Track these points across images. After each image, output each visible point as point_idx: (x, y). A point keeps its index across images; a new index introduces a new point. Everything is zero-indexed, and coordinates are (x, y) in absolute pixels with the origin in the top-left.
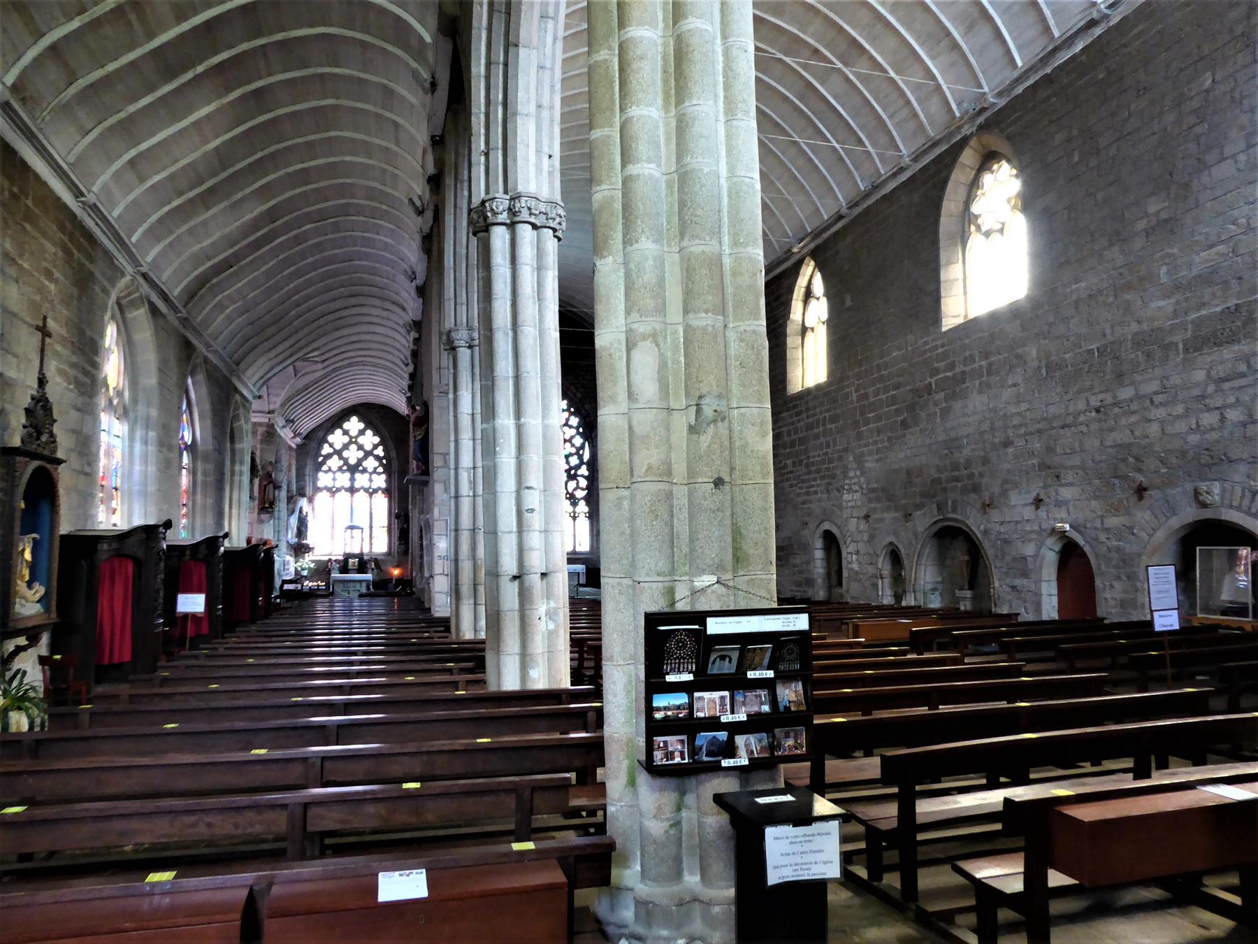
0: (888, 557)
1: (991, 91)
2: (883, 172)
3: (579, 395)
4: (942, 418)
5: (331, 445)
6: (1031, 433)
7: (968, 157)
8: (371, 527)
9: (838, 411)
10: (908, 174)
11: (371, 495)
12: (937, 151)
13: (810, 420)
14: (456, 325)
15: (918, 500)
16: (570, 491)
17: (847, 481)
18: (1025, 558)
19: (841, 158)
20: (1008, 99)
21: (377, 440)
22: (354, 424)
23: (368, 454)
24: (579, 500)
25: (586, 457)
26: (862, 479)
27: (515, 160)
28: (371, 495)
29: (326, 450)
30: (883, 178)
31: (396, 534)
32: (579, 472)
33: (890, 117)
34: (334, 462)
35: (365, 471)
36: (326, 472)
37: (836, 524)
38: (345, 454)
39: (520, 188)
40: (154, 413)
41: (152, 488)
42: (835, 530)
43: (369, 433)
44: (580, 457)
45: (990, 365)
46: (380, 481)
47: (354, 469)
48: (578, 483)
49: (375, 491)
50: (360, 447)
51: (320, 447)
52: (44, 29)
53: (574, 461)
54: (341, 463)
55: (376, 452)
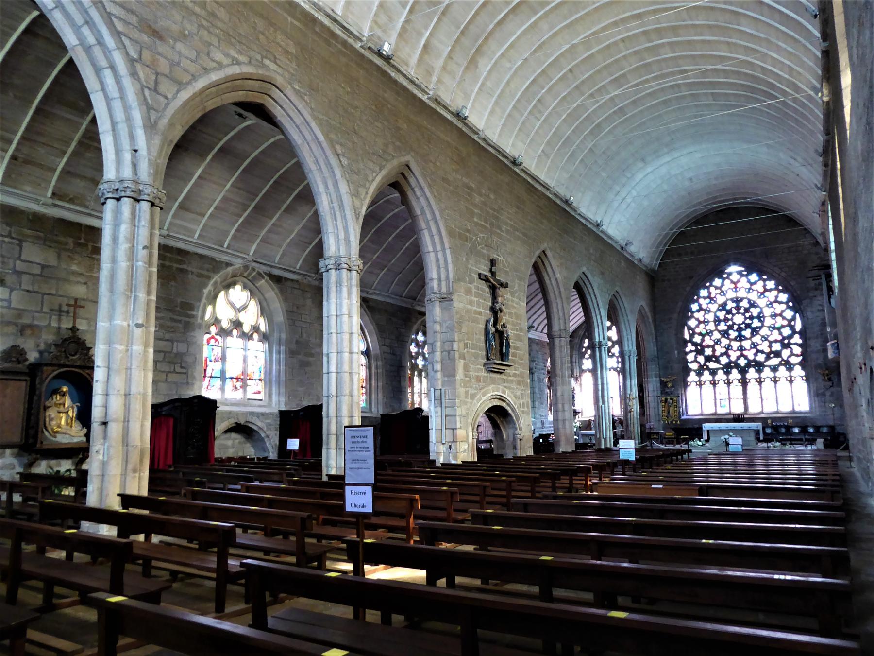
3: (783, 274)
16: (785, 359)
24: (794, 365)
25: (798, 326)
32: (792, 341)
40: (284, 336)
41: (283, 378)
44: (792, 328)
48: (791, 351)
52: (54, 167)
53: (787, 332)
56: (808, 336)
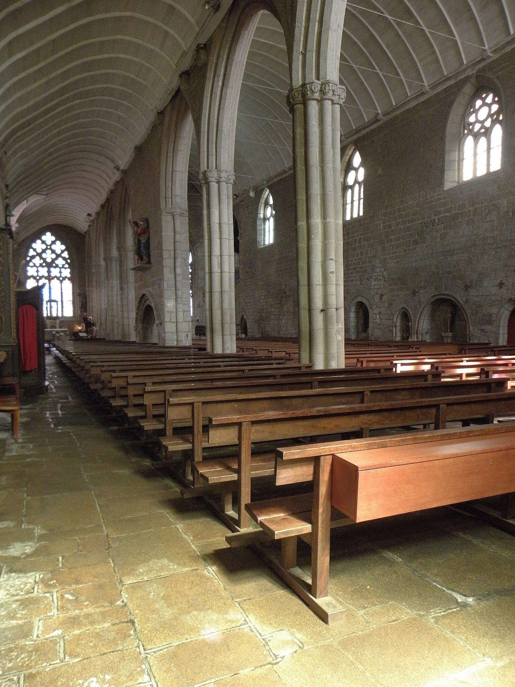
0: (400, 315)
1: (490, 48)
2: (409, 95)
4: (441, 239)
5: (35, 250)
6: (500, 248)
7: (468, 89)
8: (62, 301)
9: (370, 235)
10: (426, 97)
11: (61, 282)
12: (448, 84)
13: (350, 240)
14: (208, 168)
15: (423, 284)
17: (374, 274)
18: (491, 315)
19: (383, 85)
20: (499, 55)
21: (63, 247)
22: (48, 237)
23: (58, 256)
26: (385, 273)
27: (326, 59)
28: (61, 282)
29: (31, 253)
30: (409, 98)
31: (79, 305)
33: (420, 61)
34: (37, 261)
35: (57, 266)
36: (32, 267)
37: (366, 298)
38: (44, 255)
39: (328, 78)
42: (365, 301)
43: (58, 243)
45: (476, 210)
46: (67, 273)
47: (50, 265)
49: (64, 279)
50: (53, 252)
51: (28, 251)
54: (42, 261)
55: (63, 255)
56: (197, 267)
